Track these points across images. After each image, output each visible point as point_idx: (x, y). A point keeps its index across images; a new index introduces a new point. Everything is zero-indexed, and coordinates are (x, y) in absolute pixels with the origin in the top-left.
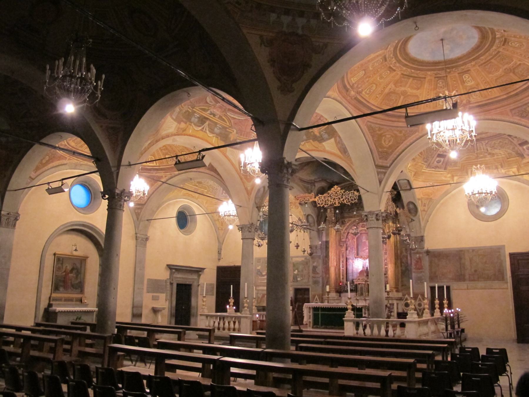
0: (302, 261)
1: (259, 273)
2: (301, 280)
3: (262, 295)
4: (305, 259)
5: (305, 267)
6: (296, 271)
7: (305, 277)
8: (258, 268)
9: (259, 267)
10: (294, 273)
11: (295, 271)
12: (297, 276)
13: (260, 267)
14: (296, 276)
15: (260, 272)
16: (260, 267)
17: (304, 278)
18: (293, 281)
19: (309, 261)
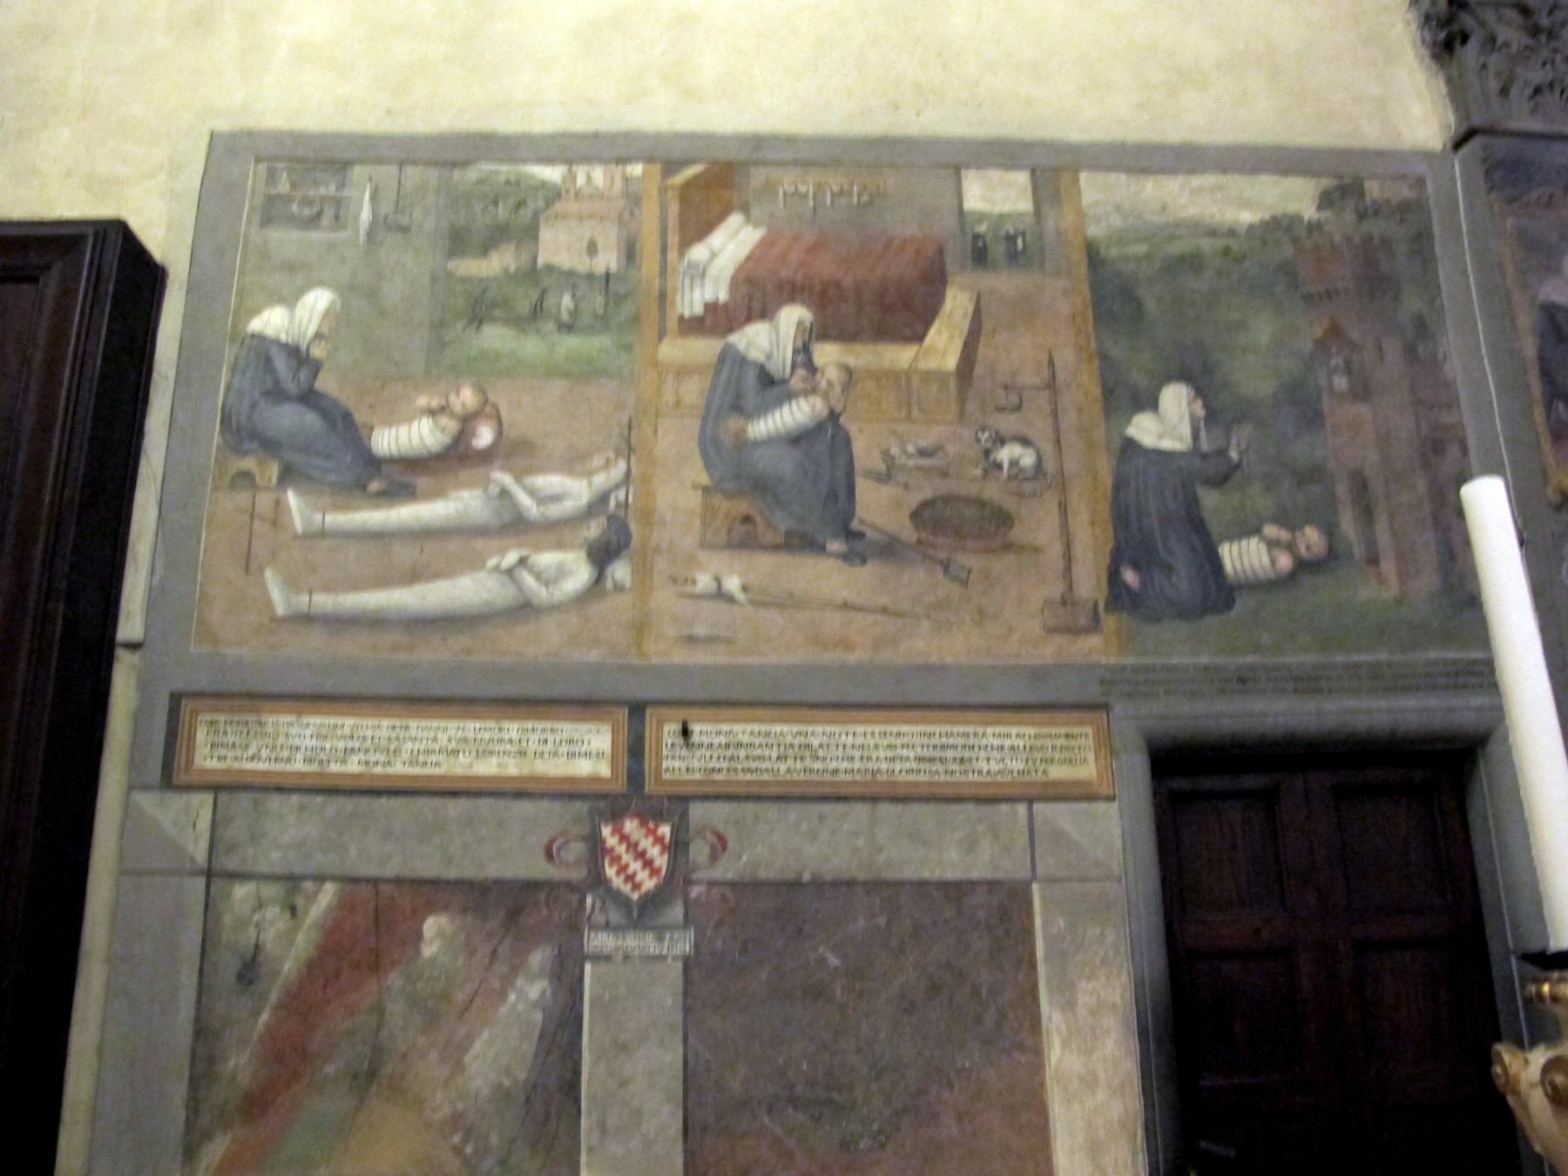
0: (1279, 227)
1: (288, 419)
2: (1304, 566)
3: (328, 894)
4: (1326, 200)
5: (1335, 332)
6: (1176, 399)
7: (1366, 513)
8: (271, 321)
9: (290, 300)
10: (1130, 446)
11: (1150, 403)
12: (1210, 499)
13: (318, 301)
14: (1192, 504)
15: (309, 397)
16: (318, 301)
17: (1348, 525)
18: (1118, 596)
19: (1422, 241)
